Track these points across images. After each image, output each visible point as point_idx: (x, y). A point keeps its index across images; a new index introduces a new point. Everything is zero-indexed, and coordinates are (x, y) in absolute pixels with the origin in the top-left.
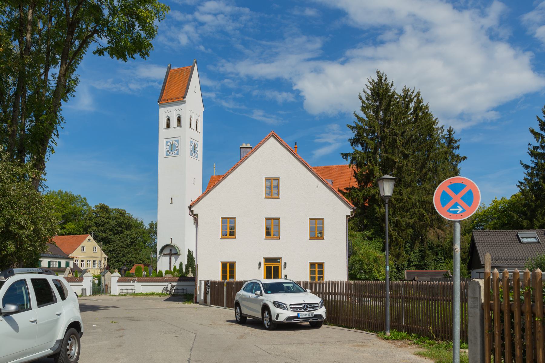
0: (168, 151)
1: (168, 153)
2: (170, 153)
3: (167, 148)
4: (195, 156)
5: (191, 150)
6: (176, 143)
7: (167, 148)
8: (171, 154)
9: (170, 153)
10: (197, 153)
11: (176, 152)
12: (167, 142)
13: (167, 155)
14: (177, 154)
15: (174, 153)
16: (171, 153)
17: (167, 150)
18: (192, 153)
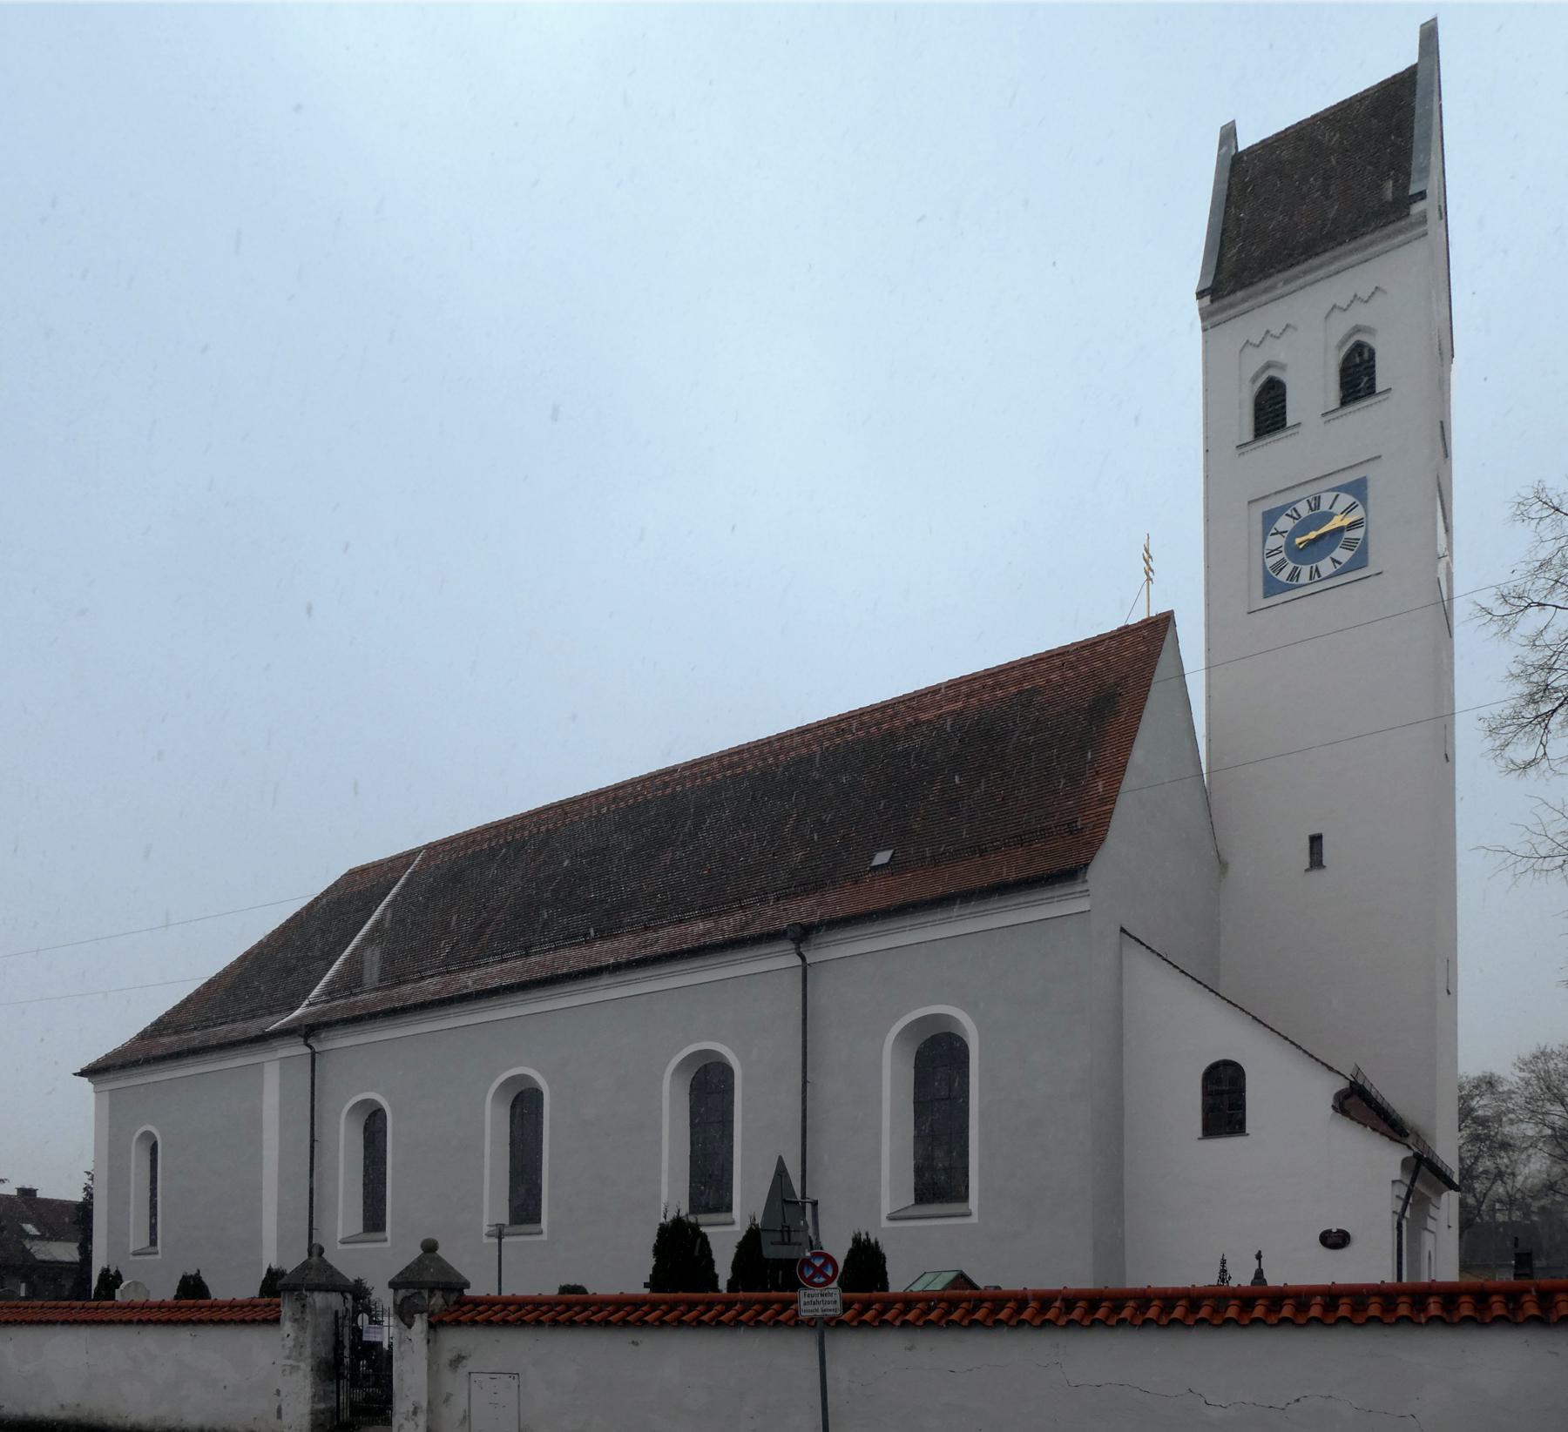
0: (1279, 567)
1: (1283, 576)
2: (1294, 574)
3: (1271, 554)
7: (1271, 554)
8: (1304, 578)
9: (1294, 574)
13: (1272, 587)
17: (1271, 562)
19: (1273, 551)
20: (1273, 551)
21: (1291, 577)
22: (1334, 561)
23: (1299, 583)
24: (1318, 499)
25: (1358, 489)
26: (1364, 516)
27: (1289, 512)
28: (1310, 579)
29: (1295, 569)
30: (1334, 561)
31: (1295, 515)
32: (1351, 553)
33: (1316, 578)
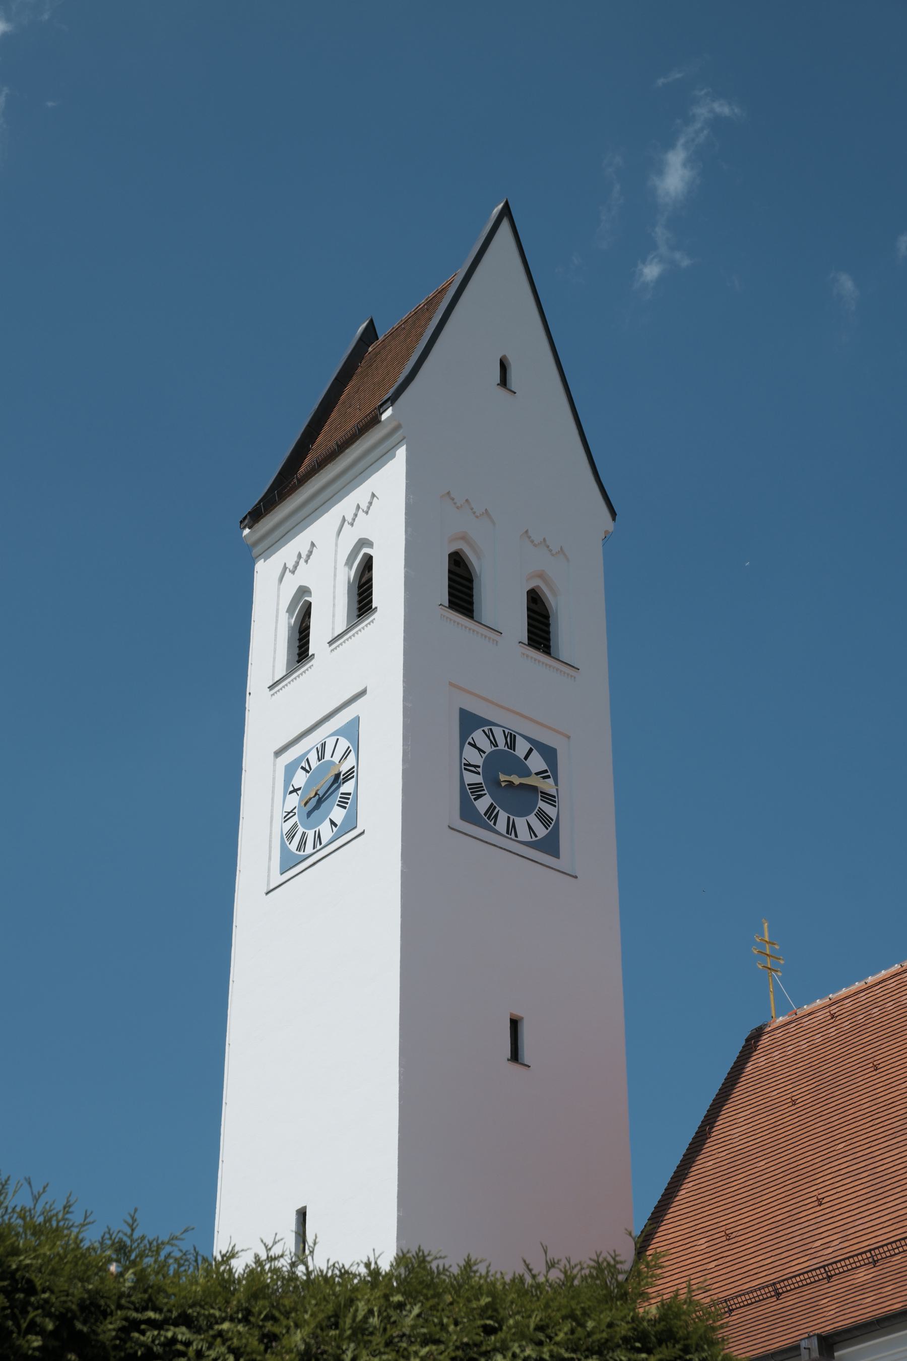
0: (291, 835)
1: (293, 847)
2: (302, 845)
4: (524, 834)
5: (471, 778)
6: (344, 744)
8: (309, 849)
9: (302, 845)
10: (544, 818)
11: (338, 814)
12: (290, 771)
13: (289, 862)
14: (351, 823)
15: (326, 831)
16: (311, 834)
18: (482, 805)
19: (289, 813)
20: (289, 813)
21: (299, 849)
22: (333, 823)
23: (554, 819)
24: (324, 745)
25: (352, 731)
26: (355, 764)
27: (303, 764)
28: (314, 848)
29: (304, 834)
30: (333, 823)
31: (308, 768)
32: (345, 811)
33: (319, 847)
